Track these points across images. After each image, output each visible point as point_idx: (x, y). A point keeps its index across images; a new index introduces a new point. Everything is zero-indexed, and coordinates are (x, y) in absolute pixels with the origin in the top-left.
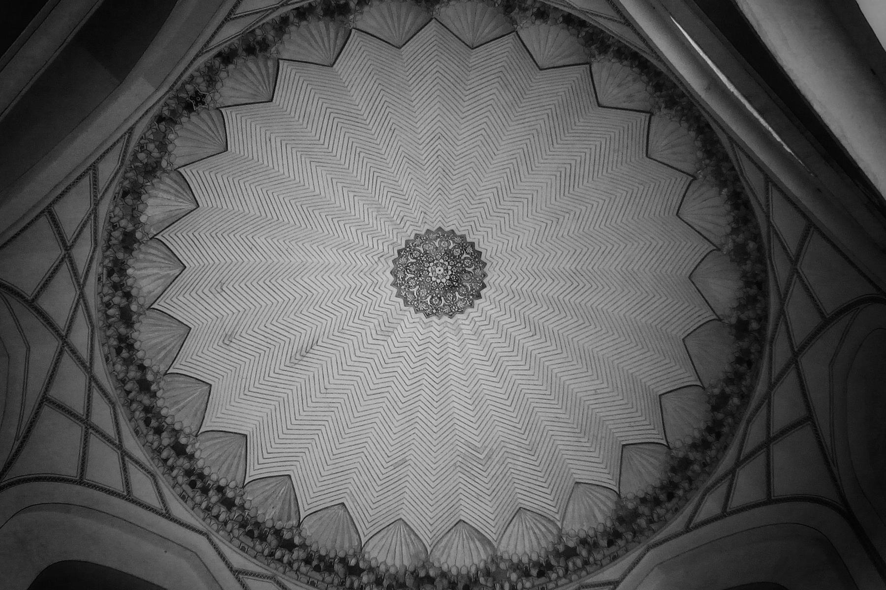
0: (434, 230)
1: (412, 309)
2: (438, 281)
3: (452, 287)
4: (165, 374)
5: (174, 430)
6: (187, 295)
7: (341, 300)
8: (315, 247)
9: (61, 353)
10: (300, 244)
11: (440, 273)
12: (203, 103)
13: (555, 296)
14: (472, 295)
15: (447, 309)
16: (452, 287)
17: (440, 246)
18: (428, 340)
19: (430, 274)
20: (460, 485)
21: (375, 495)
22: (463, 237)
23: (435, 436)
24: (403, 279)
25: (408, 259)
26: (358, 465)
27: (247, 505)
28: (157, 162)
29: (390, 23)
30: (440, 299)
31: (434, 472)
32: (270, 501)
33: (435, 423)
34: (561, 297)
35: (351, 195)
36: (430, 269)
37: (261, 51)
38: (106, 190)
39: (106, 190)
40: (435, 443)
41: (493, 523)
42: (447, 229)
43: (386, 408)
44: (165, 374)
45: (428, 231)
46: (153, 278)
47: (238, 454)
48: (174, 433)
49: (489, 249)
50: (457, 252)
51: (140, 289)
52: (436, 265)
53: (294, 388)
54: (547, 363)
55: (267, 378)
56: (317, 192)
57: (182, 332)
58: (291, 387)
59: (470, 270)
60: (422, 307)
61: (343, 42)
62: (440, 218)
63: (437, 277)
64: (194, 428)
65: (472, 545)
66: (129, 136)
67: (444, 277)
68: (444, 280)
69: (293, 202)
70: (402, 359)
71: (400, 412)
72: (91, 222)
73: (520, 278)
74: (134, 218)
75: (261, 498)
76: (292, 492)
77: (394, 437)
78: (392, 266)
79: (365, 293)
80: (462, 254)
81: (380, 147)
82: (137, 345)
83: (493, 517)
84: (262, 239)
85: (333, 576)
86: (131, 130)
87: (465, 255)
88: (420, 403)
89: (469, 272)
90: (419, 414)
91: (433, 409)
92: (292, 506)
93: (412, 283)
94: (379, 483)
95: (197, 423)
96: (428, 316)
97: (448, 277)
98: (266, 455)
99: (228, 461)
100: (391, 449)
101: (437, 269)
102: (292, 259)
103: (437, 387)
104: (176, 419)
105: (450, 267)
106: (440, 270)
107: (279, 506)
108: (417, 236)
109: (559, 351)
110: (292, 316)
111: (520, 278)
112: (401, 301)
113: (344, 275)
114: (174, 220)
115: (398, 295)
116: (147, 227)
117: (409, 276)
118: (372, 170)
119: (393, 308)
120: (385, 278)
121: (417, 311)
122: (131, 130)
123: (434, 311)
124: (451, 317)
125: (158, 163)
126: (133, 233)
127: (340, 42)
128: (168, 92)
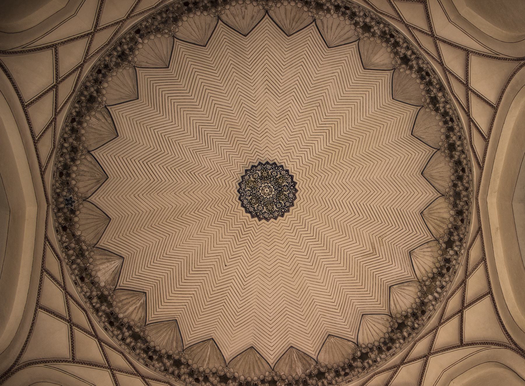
0: (244, 174)
1: (272, 220)
2: (271, 196)
3: (280, 192)
4: (183, 351)
5: (213, 374)
6: (160, 307)
7: (236, 247)
8: (199, 233)
9: (114, 376)
10: (191, 238)
11: (268, 191)
12: (74, 202)
13: (325, 146)
14: (292, 186)
15: (288, 204)
16: (280, 192)
17: (255, 179)
18: (294, 226)
19: (265, 196)
20: (375, 273)
21: (341, 318)
22: (260, 163)
23: (342, 265)
24: (255, 210)
25: (247, 199)
26: (320, 313)
27: (284, 377)
28: (80, 250)
29: (122, 91)
30: (280, 203)
31: (358, 281)
32: (294, 366)
33: (336, 259)
34: (328, 144)
35: (191, 193)
36: (262, 194)
37: (75, 153)
38: (63, 278)
39: (63, 278)
40: (345, 268)
41: (406, 273)
42: (250, 168)
43: (306, 275)
44: (183, 351)
45: (242, 177)
46: (136, 311)
47: (257, 359)
48: (215, 375)
49: (277, 157)
50: (265, 174)
51: (133, 320)
52: (262, 190)
53: (255, 307)
54: (354, 179)
55: (238, 314)
56: (174, 206)
57: (174, 325)
58: (253, 307)
59: (279, 176)
60: (276, 214)
61: (110, 119)
62: (241, 166)
63: (269, 195)
64: (223, 365)
65: (407, 292)
66: (49, 242)
67: (271, 191)
68: (273, 193)
69: (168, 221)
70: (291, 246)
71: (315, 271)
72: (71, 302)
73: (303, 155)
74: (98, 288)
75: (287, 368)
76: (301, 353)
77: (324, 284)
78: (243, 209)
79: (244, 233)
80: (268, 173)
81: (181, 158)
82: (158, 348)
83: (403, 271)
84: (171, 250)
85: (356, 370)
86: (46, 238)
87: (270, 172)
88: (319, 258)
89: (280, 177)
90: (324, 263)
91: (328, 254)
92: (307, 359)
93: (260, 208)
94: (338, 311)
95: (222, 362)
96: (282, 216)
97: (274, 190)
98: (272, 349)
99: (256, 367)
100: (328, 291)
101: (265, 191)
102: (194, 248)
103: (319, 242)
104: (211, 366)
105: (270, 185)
106: (267, 191)
107: (299, 364)
108: (239, 184)
109: (353, 168)
110: (221, 275)
111: (303, 155)
112: (263, 221)
113: (226, 234)
114: (118, 273)
115: (260, 219)
116: (108, 287)
117: (256, 206)
118: (188, 172)
119: (263, 228)
120: (247, 218)
121: (276, 218)
122: (46, 238)
123: (283, 210)
124: (293, 205)
125: (81, 249)
126: (102, 294)
127: (109, 119)
128: (48, 206)
